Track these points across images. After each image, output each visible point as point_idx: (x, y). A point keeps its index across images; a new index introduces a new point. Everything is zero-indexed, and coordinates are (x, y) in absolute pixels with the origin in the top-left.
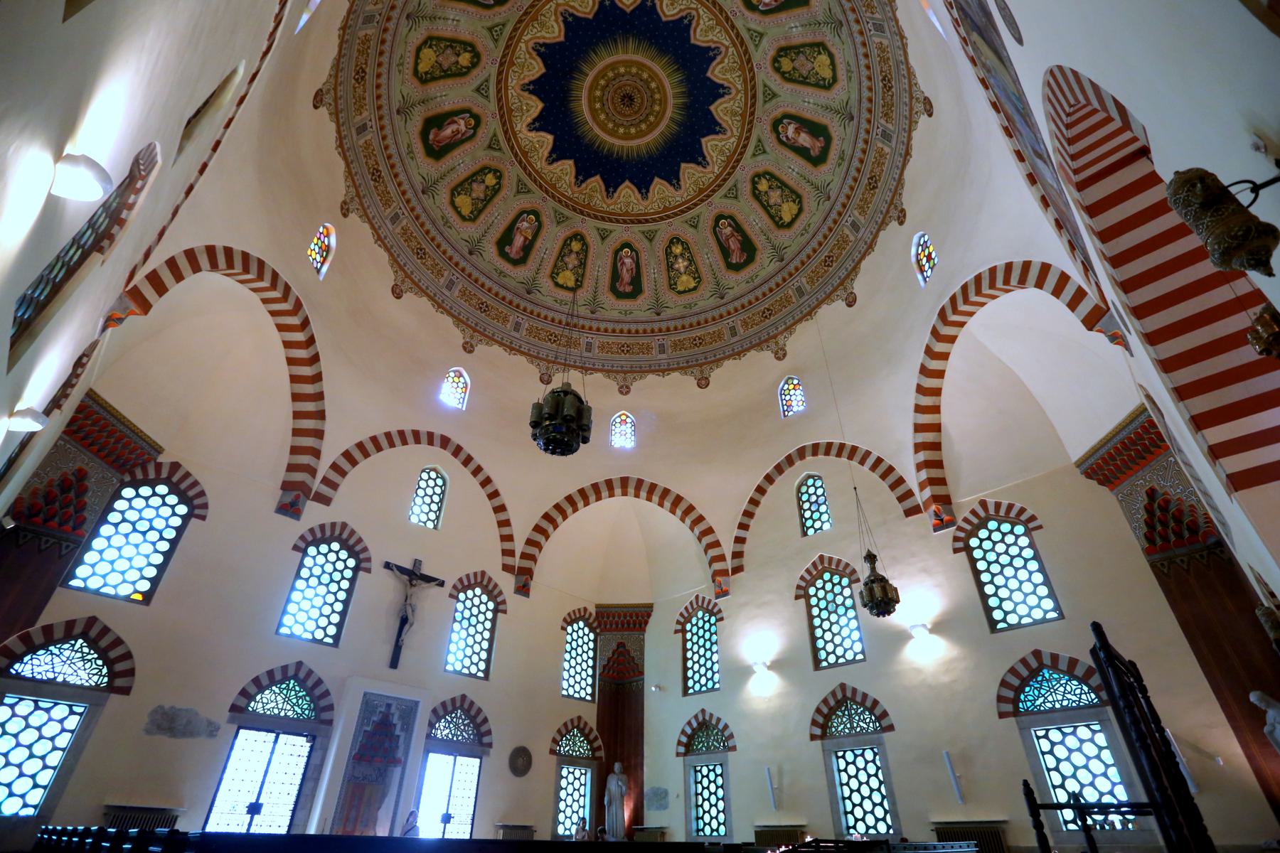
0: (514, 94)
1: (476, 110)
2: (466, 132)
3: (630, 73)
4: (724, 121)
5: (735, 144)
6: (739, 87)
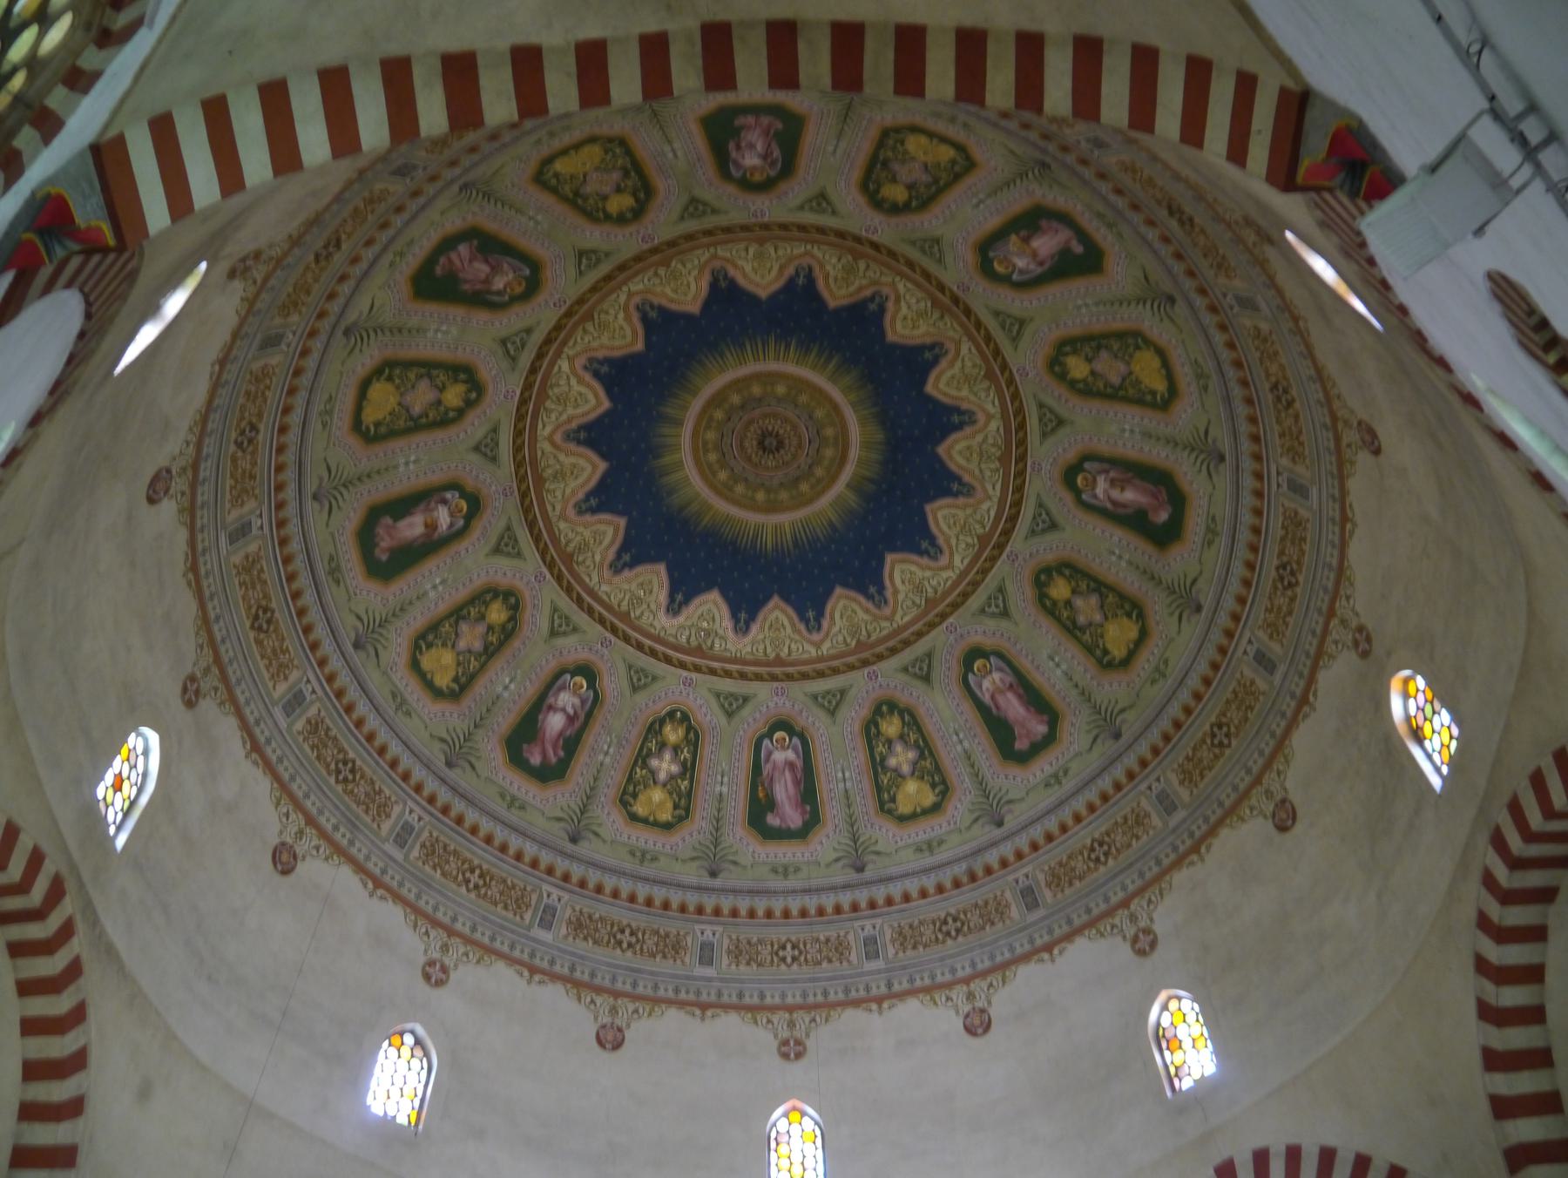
0: (989, 488)
1: (1068, 497)
2: (1100, 472)
3: (768, 491)
6: (562, 525)
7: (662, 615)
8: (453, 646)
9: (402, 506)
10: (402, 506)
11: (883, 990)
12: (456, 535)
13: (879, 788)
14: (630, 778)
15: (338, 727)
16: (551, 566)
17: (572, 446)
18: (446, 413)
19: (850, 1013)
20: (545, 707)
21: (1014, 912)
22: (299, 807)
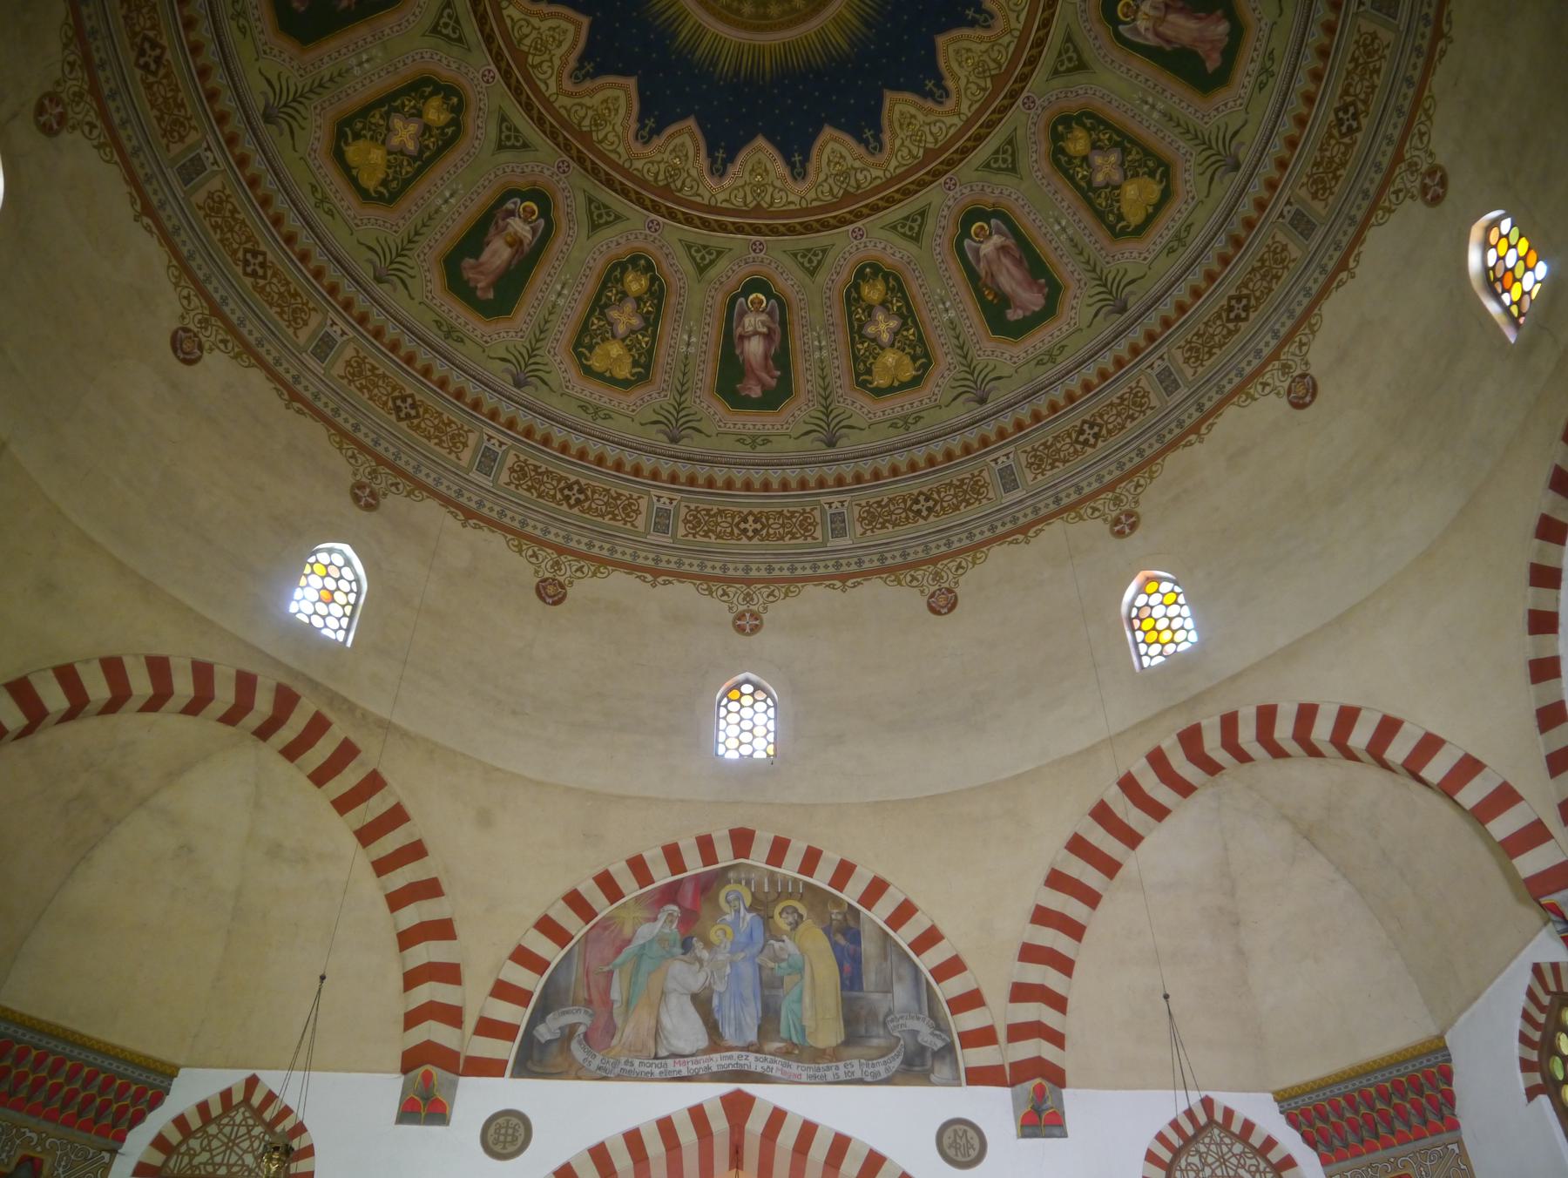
4: (593, 92)
5: (543, 87)
6: (638, 164)
7: (709, 180)
8: (614, 337)
9: (474, 240)
10: (474, 240)
11: (1196, 415)
12: (544, 239)
13: (1100, 215)
14: (856, 358)
15: (542, 461)
16: (655, 208)
17: (588, 84)
18: (443, 133)
19: (1171, 458)
20: (736, 341)
21: (1294, 252)
22: (543, 544)
